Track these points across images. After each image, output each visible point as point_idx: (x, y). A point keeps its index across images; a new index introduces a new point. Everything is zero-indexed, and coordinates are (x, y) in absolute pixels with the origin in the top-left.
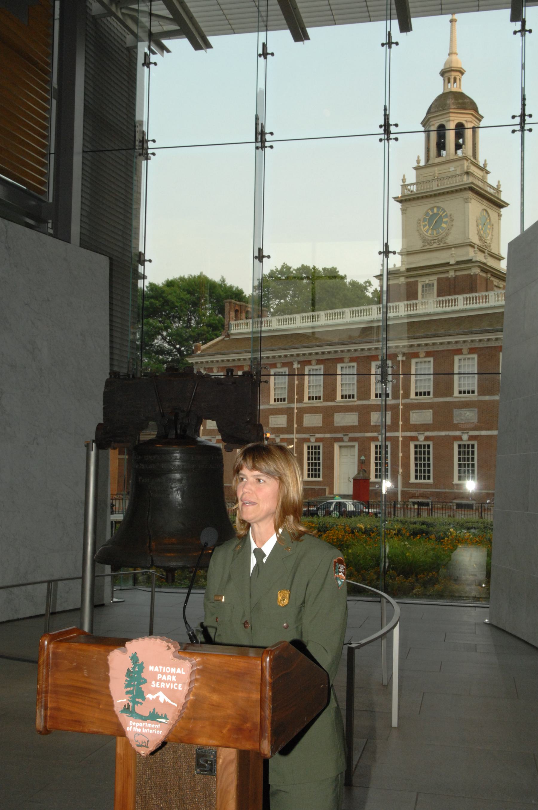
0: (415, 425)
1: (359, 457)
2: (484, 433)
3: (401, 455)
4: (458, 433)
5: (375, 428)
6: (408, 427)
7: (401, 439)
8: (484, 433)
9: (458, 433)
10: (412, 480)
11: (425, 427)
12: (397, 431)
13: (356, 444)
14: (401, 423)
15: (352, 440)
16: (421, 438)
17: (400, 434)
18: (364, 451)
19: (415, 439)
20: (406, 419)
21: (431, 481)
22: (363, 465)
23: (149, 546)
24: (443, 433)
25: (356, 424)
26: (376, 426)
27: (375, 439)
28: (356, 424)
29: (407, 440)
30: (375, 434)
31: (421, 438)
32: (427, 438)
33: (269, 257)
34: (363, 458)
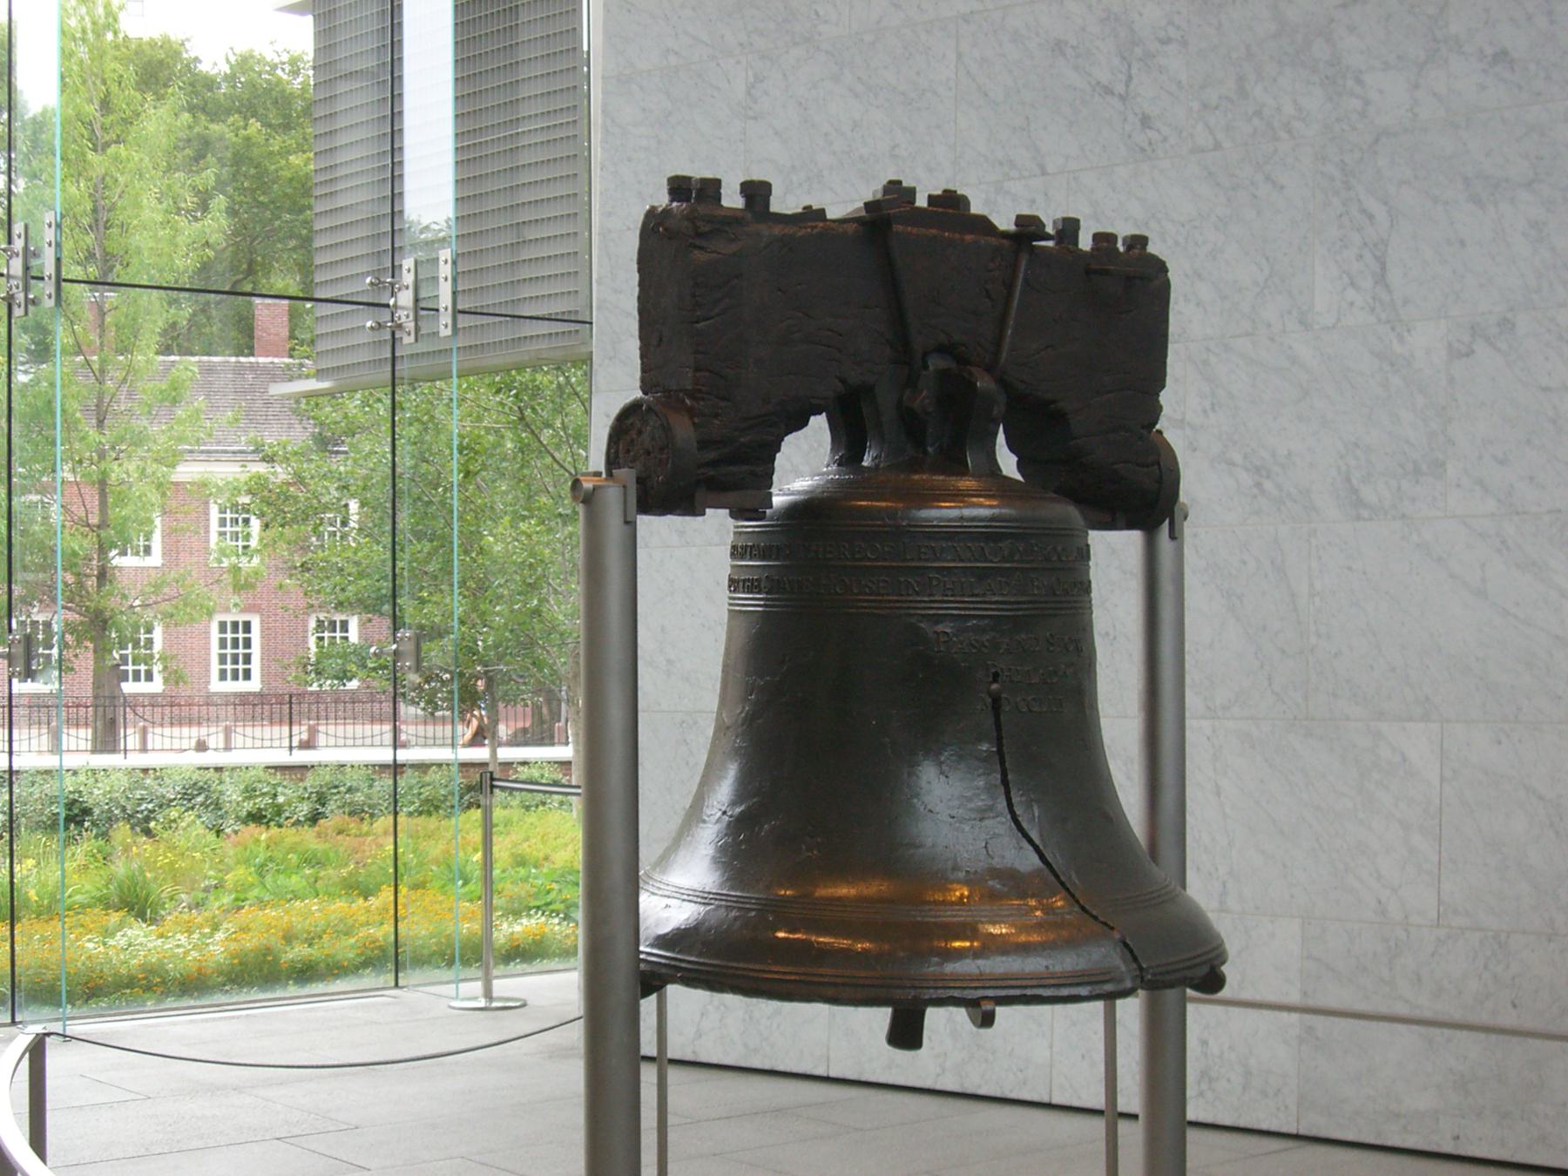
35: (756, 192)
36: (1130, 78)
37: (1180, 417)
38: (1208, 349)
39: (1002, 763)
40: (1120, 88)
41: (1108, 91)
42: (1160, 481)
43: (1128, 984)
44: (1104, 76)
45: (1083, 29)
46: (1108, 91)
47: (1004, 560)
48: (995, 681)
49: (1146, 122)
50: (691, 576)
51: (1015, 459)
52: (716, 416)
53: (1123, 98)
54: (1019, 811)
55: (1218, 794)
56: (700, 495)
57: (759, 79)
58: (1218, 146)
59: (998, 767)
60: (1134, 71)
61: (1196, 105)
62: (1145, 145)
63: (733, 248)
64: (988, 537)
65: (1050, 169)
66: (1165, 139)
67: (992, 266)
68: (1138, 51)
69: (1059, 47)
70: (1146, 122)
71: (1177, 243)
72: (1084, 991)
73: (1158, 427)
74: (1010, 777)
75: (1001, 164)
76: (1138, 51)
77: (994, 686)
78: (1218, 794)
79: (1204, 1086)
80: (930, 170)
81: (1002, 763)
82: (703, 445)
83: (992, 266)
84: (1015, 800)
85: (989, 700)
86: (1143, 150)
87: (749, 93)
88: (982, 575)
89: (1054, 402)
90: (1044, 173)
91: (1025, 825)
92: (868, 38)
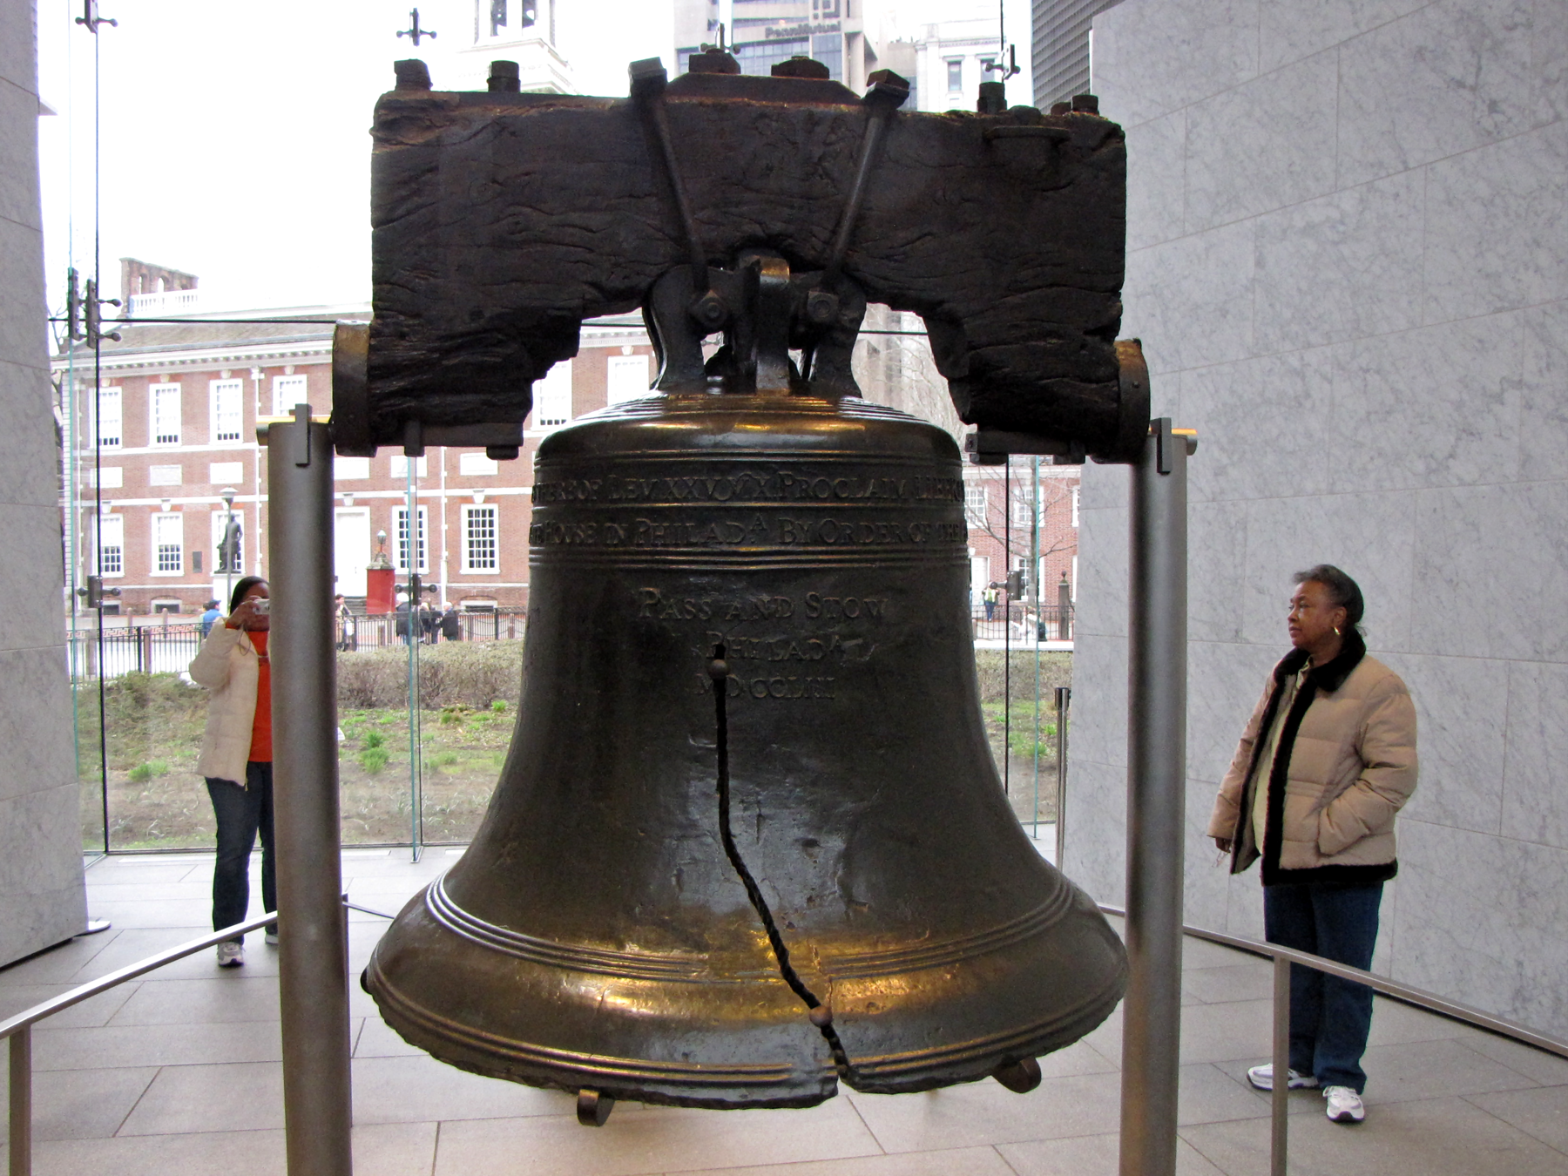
1: (373, 532)
3: (444, 527)
5: (399, 484)
7: (444, 501)
10: (465, 569)
12: (437, 486)
13: (366, 510)
14: (444, 474)
15: (358, 502)
16: (479, 498)
17: (443, 494)
18: (379, 521)
19: (468, 500)
21: (496, 570)
22: (380, 544)
23: (788, 974)
26: (400, 479)
27: (399, 501)
30: (398, 494)
31: (479, 498)
32: (488, 499)
33: (433, 35)
34: (382, 533)
35: (504, 75)
36: (1479, 69)
37: (1516, 378)
38: (1545, 313)
39: (723, 763)
40: (1470, 81)
41: (1461, 84)
42: (1118, 398)
43: (815, 1089)
44: (1456, 72)
45: (1440, 33)
46: (1461, 84)
47: (736, 497)
48: (720, 652)
49: (1493, 107)
50: (446, 526)
51: (945, 381)
52: (403, 336)
53: (1473, 89)
54: (735, 828)
55: (1542, 733)
56: (412, 430)
57: (1195, 125)
58: (1558, 117)
59: (716, 771)
60: (1484, 62)
61: (1538, 83)
62: (1491, 129)
63: (430, 136)
64: (714, 467)
65: (1411, 165)
66: (1510, 120)
67: (833, 137)
68: (1488, 42)
69: (1420, 53)
70: (1493, 107)
71: (1518, 216)
72: (731, 1095)
73: (1124, 334)
74: (732, 783)
75: (1372, 165)
76: (1488, 42)
77: (720, 664)
78: (1542, 733)
79: (1518, 1004)
80: (1318, 180)
81: (723, 763)
82: (377, 371)
83: (833, 137)
84: (735, 811)
85: (708, 682)
86: (1490, 133)
87: (1187, 137)
88: (703, 517)
89: (941, 303)
90: (1407, 169)
91: (740, 850)
92: (1272, 76)
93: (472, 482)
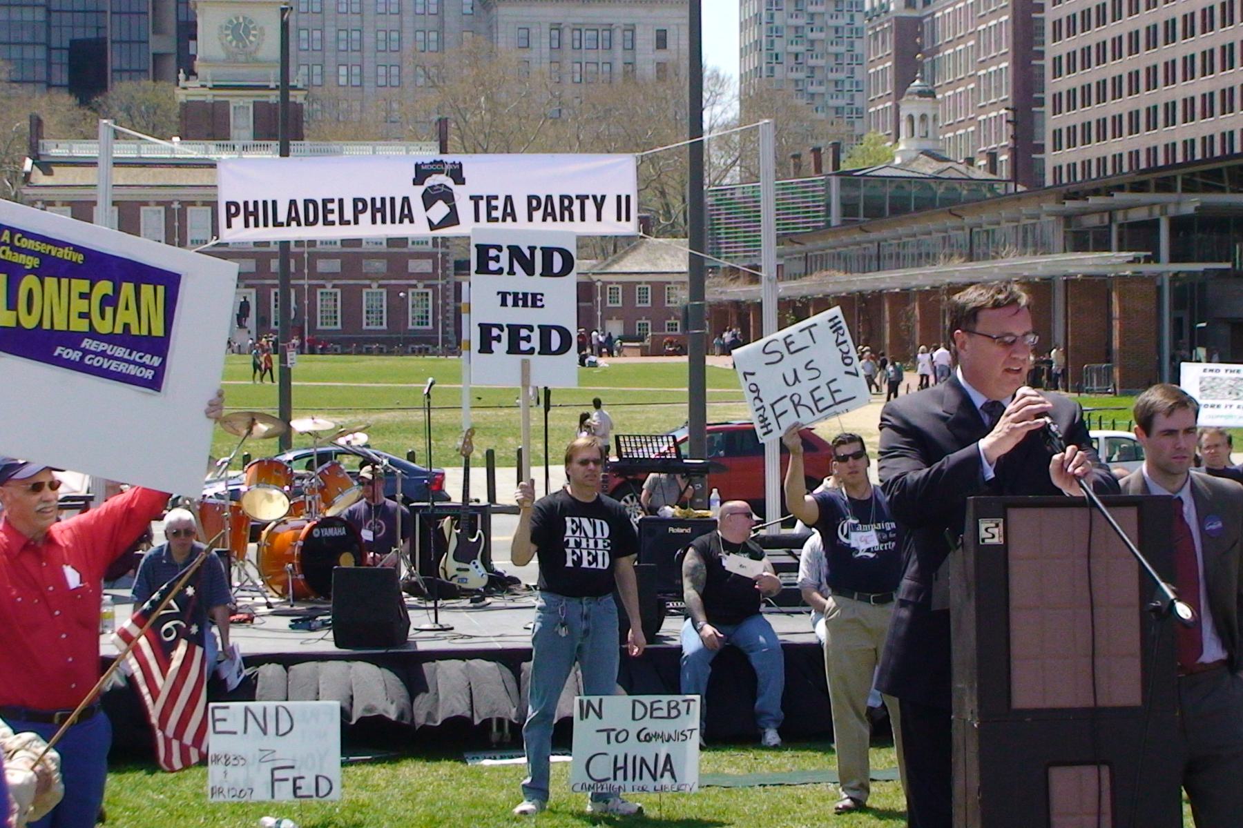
0: (322, 273)
2: (393, 282)
3: (306, 302)
4: (367, 282)
6: (313, 274)
8: (393, 282)
9: (367, 282)
10: (319, 326)
11: (334, 276)
14: (306, 271)
17: (305, 282)
20: (312, 267)
24: (351, 282)
25: (254, 270)
28: (254, 270)
29: (313, 288)
93: (324, 276)
